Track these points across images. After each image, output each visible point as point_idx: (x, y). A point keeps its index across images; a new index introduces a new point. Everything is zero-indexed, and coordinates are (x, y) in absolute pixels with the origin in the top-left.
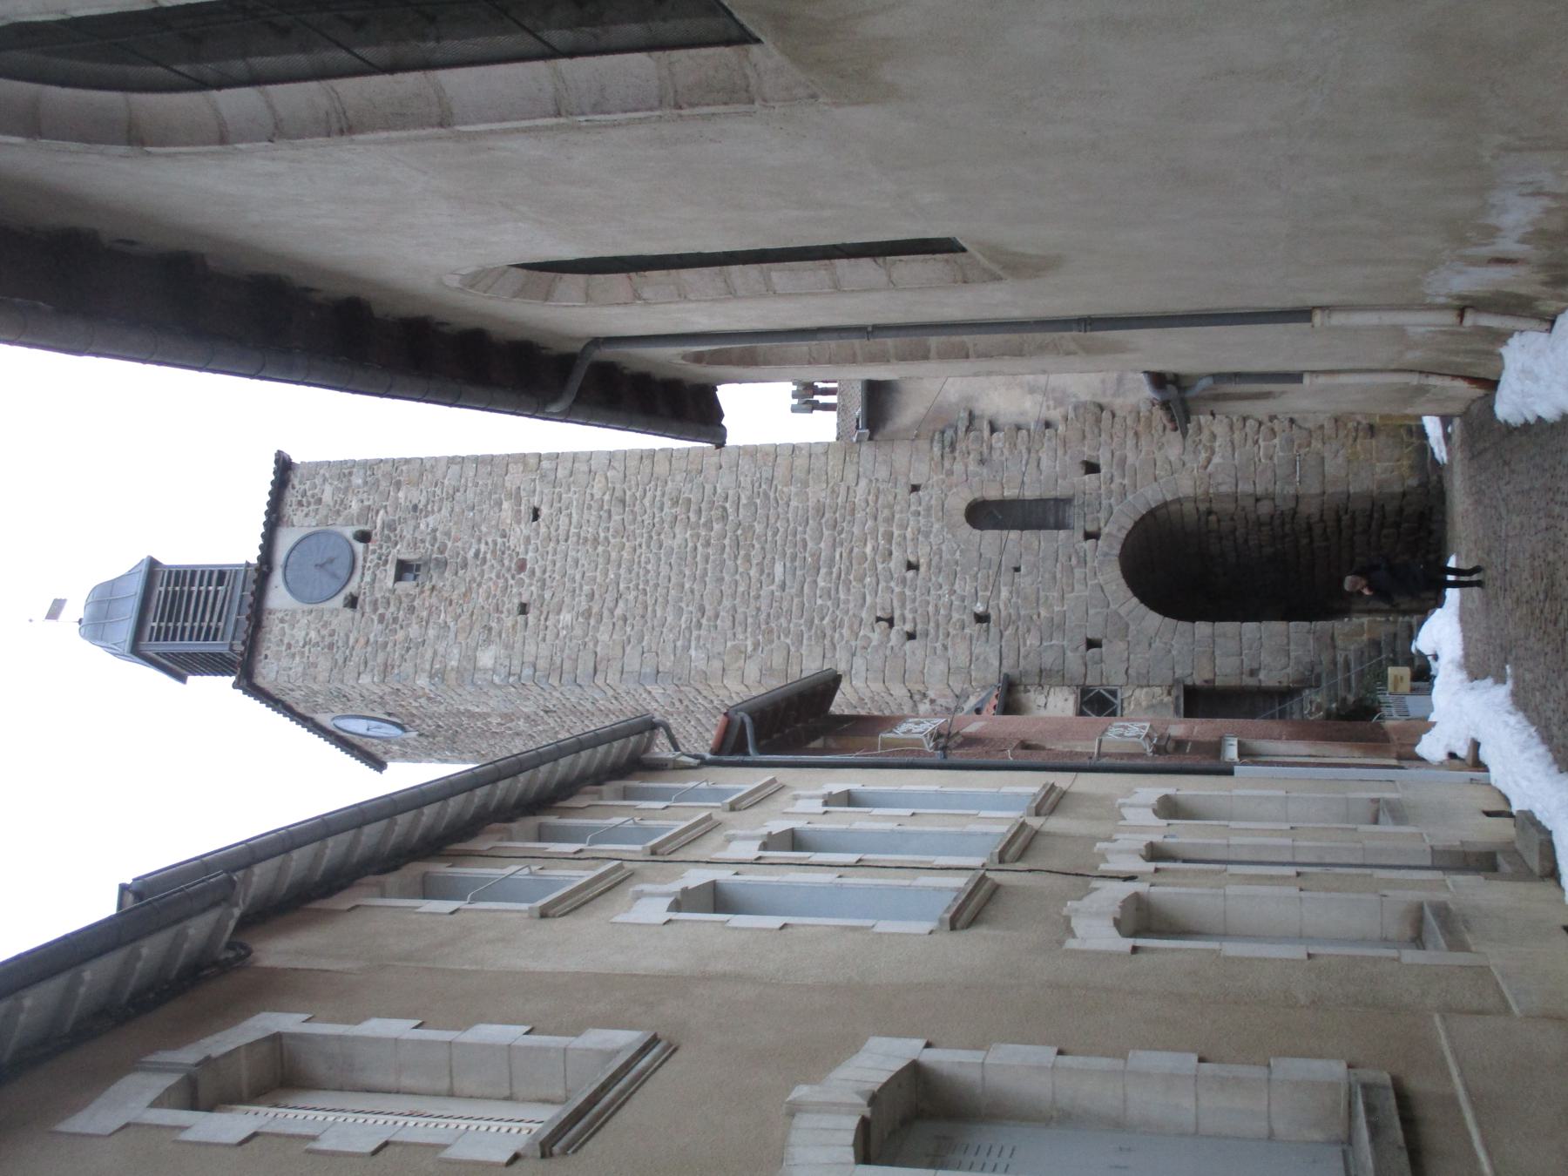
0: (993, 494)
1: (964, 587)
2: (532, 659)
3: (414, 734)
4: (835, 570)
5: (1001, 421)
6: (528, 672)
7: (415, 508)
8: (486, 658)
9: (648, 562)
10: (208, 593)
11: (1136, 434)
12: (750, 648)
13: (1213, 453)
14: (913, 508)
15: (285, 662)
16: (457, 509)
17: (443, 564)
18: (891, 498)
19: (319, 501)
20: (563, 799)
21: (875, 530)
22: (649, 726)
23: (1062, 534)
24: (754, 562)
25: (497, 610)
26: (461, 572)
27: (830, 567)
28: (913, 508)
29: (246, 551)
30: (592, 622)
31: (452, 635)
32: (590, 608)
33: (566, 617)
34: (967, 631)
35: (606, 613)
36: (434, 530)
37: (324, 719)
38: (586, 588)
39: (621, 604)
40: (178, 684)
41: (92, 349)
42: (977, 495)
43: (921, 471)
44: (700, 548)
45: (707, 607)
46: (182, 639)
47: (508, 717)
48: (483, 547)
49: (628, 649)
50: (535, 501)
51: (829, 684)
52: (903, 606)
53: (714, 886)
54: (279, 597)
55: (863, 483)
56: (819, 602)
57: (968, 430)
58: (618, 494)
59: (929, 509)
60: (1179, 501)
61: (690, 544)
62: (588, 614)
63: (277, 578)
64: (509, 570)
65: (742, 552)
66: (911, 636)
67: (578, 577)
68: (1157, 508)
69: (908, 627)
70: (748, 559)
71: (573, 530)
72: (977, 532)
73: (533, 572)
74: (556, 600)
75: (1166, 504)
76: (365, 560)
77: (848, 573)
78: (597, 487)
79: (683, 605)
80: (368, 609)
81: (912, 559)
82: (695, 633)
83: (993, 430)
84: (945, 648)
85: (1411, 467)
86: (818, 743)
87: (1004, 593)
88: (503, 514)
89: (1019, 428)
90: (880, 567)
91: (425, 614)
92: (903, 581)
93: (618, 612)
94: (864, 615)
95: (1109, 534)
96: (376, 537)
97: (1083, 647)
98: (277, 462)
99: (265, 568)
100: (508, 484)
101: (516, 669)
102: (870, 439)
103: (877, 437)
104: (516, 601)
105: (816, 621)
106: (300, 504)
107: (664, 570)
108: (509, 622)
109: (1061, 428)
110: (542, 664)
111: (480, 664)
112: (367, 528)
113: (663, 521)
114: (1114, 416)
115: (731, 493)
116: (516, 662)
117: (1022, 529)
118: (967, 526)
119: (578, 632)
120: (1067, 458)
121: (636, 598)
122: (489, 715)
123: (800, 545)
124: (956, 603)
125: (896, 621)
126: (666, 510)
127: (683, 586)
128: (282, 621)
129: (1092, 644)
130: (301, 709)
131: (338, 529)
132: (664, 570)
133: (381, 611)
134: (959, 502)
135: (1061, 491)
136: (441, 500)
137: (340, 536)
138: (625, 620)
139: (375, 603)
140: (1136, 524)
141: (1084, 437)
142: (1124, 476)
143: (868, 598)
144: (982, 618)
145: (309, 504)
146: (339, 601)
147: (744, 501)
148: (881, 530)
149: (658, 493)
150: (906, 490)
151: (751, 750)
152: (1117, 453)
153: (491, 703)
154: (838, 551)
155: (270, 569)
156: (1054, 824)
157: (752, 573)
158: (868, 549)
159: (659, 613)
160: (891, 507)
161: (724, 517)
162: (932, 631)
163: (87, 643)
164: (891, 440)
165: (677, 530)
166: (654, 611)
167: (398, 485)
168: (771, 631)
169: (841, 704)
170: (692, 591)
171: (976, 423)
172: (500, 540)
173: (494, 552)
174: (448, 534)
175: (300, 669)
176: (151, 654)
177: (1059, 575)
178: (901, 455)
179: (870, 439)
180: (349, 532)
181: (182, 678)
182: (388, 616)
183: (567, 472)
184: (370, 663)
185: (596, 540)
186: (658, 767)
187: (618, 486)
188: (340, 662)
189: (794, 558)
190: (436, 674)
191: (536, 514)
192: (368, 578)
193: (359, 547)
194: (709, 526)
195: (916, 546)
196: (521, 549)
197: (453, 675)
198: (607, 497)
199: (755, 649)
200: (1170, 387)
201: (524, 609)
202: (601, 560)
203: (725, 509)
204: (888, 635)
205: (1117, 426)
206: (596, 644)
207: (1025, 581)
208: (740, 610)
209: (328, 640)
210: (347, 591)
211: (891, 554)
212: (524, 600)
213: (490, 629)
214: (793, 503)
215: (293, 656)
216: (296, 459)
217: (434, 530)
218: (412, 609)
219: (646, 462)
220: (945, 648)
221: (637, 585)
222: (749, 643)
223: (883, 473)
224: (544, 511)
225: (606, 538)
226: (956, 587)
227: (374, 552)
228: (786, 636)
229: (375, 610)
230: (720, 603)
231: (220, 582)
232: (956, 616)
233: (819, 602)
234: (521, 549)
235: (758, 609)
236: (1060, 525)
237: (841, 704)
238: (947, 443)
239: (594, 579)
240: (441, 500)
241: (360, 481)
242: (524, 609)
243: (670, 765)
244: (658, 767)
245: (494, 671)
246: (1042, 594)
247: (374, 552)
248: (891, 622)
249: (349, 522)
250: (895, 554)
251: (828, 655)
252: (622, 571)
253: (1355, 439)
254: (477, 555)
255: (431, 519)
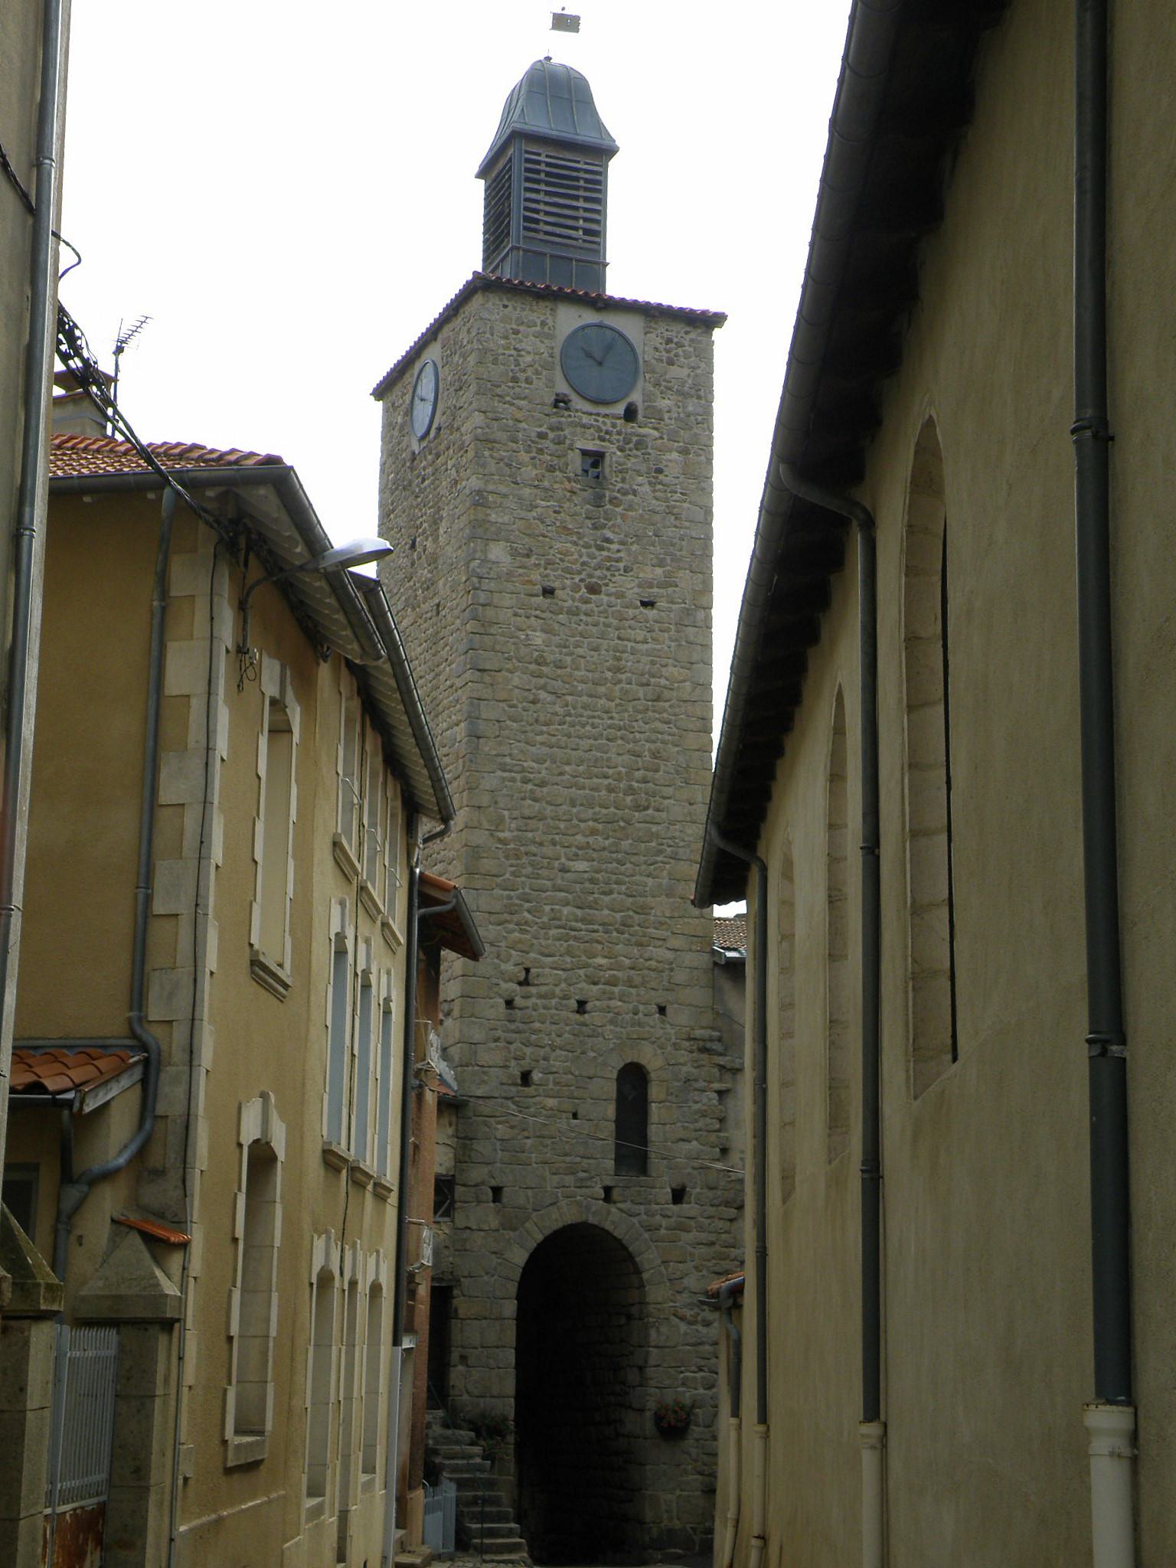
0: (655, 1091)
1: (559, 1061)
2: (495, 601)
3: (416, 447)
4: (579, 925)
5: (730, 1102)
6: (482, 597)
7: (659, 471)
8: (498, 552)
9: (594, 726)
11: (713, 1243)
12: (501, 835)
13: (690, 1323)
14: (641, 1007)
15: (499, 327)
16: (657, 518)
17: (598, 501)
18: (653, 984)
19: (671, 363)
20: (372, 720)
21: (619, 967)
22: (446, 818)
23: (610, 1164)
24: (591, 840)
25: (549, 563)
26: (589, 523)
27: (583, 920)
28: (641, 1007)
29: (616, 286)
30: (533, 667)
31: (523, 514)
32: (547, 664)
33: (538, 638)
34: (513, 1063)
35: (542, 681)
36: (635, 493)
37: (434, 353)
38: (569, 659)
39: (550, 698)
40: (476, 169)
41: (810, 281)
42: (653, 1076)
43: (681, 1018)
44: (606, 782)
45: (545, 790)
46: (526, 228)
47: (433, 560)
48: (615, 547)
50: (662, 604)
51: (470, 950)
52: (540, 996)
53: (346, 952)
54: (569, 319)
55: (669, 955)
56: (547, 908)
57: (722, 1067)
58: (666, 694)
59: (640, 1024)
60: (642, 1286)
61: (611, 771)
62: (540, 662)
63: (590, 317)
64: (590, 576)
65: (600, 827)
66: (509, 1003)
67: (580, 651)
68: (634, 1263)
69: (518, 1001)
70: (594, 832)
71: (630, 644)
72: (615, 1075)
73: (587, 602)
74: (556, 627)
75: (638, 1272)
76: (606, 416)
77: (575, 938)
78: (673, 671)
79: (548, 764)
80: (554, 420)
81: (589, 1007)
82: (518, 776)
83: (721, 1093)
84: (497, 1040)
85: (670, 1531)
86: (422, 956)
87: (551, 1102)
88: (649, 568)
89: (722, 1120)
90: (581, 972)
91: (546, 484)
92: (566, 997)
93: (543, 695)
94: (532, 955)
95: (609, 1213)
96: (631, 428)
98: (716, 314)
99: (600, 304)
100: (681, 574)
101: (486, 584)
102: (715, 964)
103: (716, 971)
104: (556, 584)
105: (527, 905)
106: (669, 341)
107: (586, 743)
108: (535, 576)
109: (719, 1166)
110: (490, 613)
111: (492, 545)
112: (640, 416)
113: (635, 742)
114: (731, 1220)
115: (664, 815)
116: (493, 585)
117: (616, 1121)
118: (622, 1065)
119: (523, 650)
120: (689, 1170)
121: (556, 714)
122: (436, 540)
123: (607, 888)
124: (542, 1052)
125: (524, 988)
126: (648, 745)
127: (568, 764)
128: (543, 324)
130: (446, 332)
131: (640, 384)
132: (586, 743)
133: (551, 435)
134: (650, 1058)
135: (655, 1163)
136: (666, 500)
137: (631, 387)
138: (533, 702)
139: (559, 428)
140: (619, 1241)
141: (711, 1189)
142: (667, 1229)
143: (550, 959)
144: (526, 1078)
145: (668, 351)
146: (563, 387)
147: (654, 828)
148: (619, 974)
149: (666, 737)
150: (661, 1001)
151: (423, 911)
152: (692, 1223)
153: (449, 549)
154: (600, 928)
155: (599, 309)
157: (579, 837)
158: (600, 961)
159: (539, 738)
160: (643, 984)
161: (638, 808)
162: (513, 1027)
163: (526, 67)
164: (714, 987)
165: (626, 757)
166: (542, 733)
167: (684, 451)
168: (518, 858)
169: (452, 961)
170: (561, 774)
171: (728, 1076)
172: (621, 565)
173: (609, 559)
174: (630, 507)
175: (491, 345)
176: (511, 152)
177: (568, 1159)
178: (699, 995)
179: (715, 964)
180: (636, 397)
181: (482, 174)
182: (546, 443)
183: (692, 638)
184: (495, 424)
185: (619, 670)
186: (410, 828)
187: (674, 694)
188: (498, 391)
189: (592, 881)
190: (482, 497)
191: (647, 604)
192: (585, 419)
193: (620, 409)
194: (630, 791)
195: (602, 1010)
196: (611, 589)
197: (481, 516)
198: (663, 682)
199: (500, 840)
200: (731, 1301)
201: (548, 592)
202: (597, 675)
203: (646, 808)
204: (511, 980)
205: (721, 1224)
206: (508, 670)
207: (563, 1123)
208: (540, 824)
209: (522, 376)
210: (573, 396)
211: (595, 984)
212: (558, 592)
213: (528, 556)
214: (650, 881)
215: (506, 338)
216: (717, 334)
217: (635, 493)
218: (551, 469)
219: (699, 724)
220: (497, 1040)
221: (570, 715)
222: (506, 835)
223: (680, 977)
224: (651, 613)
225: (620, 681)
226: (558, 1052)
227: (614, 426)
228: (513, 873)
229: (552, 429)
230: (548, 803)
231: (586, 232)
232: (528, 1051)
233: (547, 908)
234: (611, 589)
235: (541, 844)
236: (619, 1160)
237: (452, 961)
238: (708, 1045)
239: (577, 669)
240: (666, 500)
241: (690, 408)
242: (548, 592)
243: (411, 841)
244: (410, 828)
245: (485, 561)
246: (549, 1142)
247: (614, 426)
248: (525, 983)
249: (648, 397)
250: (595, 988)
251: (493, 918)
252: (585, 699)
253: (701, 1474)
254: (608, 540)
255: (647, 488)
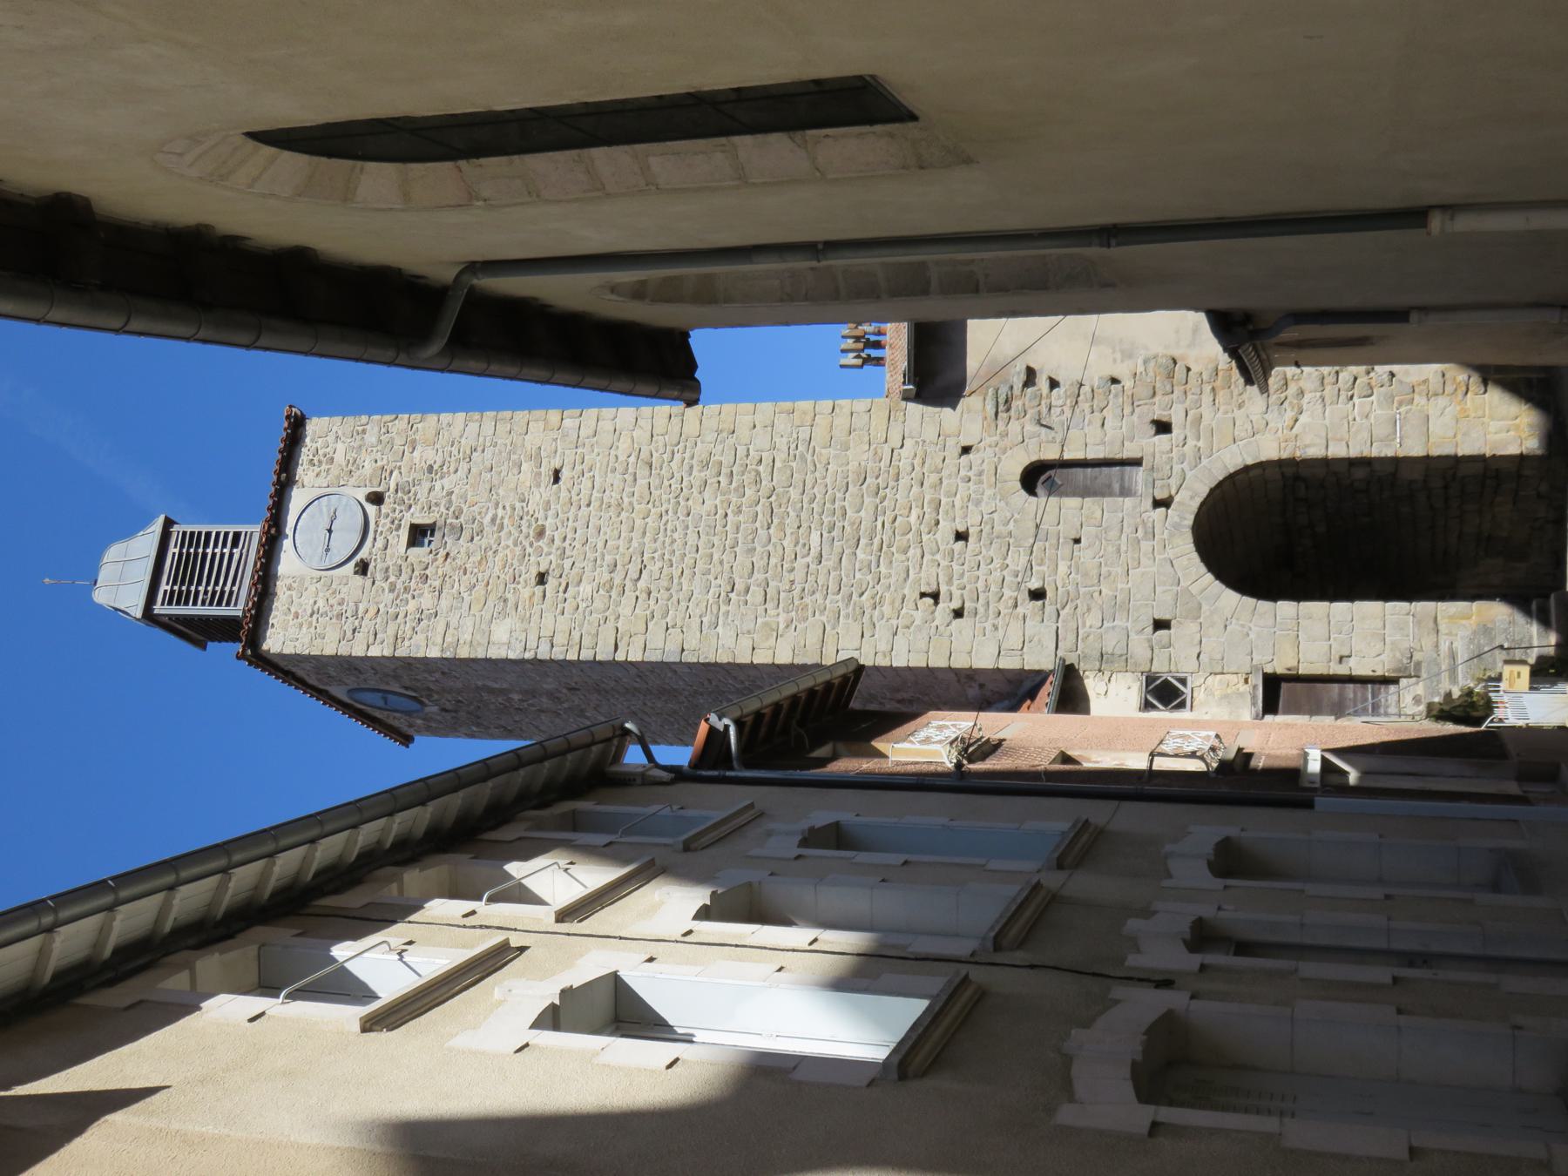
4: (877, 541)
7: (431, 467)
10: (222, 555)
12: (782, 626)
14: (963, 473)
23: (1128, 502)
30: (614, 594)
31: (466, 606)
33: (586, 589)
34: (1020, 610)
42: (1034, 458)
47: (532, 693)
48: (500, 512)
49: (650, 625)
52: (950, 581)
61: (720, 512)
66: (958, 613)
69: (956, 605)
71: (595, 494)
77: (889, 546)
78: (624, 445)
82: (723, 608)
87: (1063, 568)
90: (925, 537)
93: (642, 584)
97: (1150, 629)
107: (692, 539)
108: (525, 593)
126: (695, 473)
127: (712, 556)
129: (1160, 625)
130: (312, 681)
132: (692, 539)
140: (1212, 491)
144: (1038, 595)
149: (687, 455)
156: (1082, 884)
157: (785, 543)
161: (758, 481)
162: (981, 610)
172: (518, 505)
177: (1123, 548)
180: (361, 494)
182: (399, 586)
183: (591, 432)
186: (625, 781)
189: (832, 528)
192: (380, 543)
193: (371, 509)
196: (540, 515)
198: (632, 459)
201: (542, 579)
203: (758, 473)
207: (1085, 553)
209: (337, 609)
211: (937, 523)
212: (542, 570)
215: (301, 625)
224: (565, 474)
225: (631, 503)
231: (235, 544)
232: (1008, 593)
233: (858, 575)
234: (540, 515)
238: (1002, 400)
242: (542, 579)
246: (1104, 570)
248: (935, 596)
252: (646, 540)
254: (493, 520)
255: (446, 481)
